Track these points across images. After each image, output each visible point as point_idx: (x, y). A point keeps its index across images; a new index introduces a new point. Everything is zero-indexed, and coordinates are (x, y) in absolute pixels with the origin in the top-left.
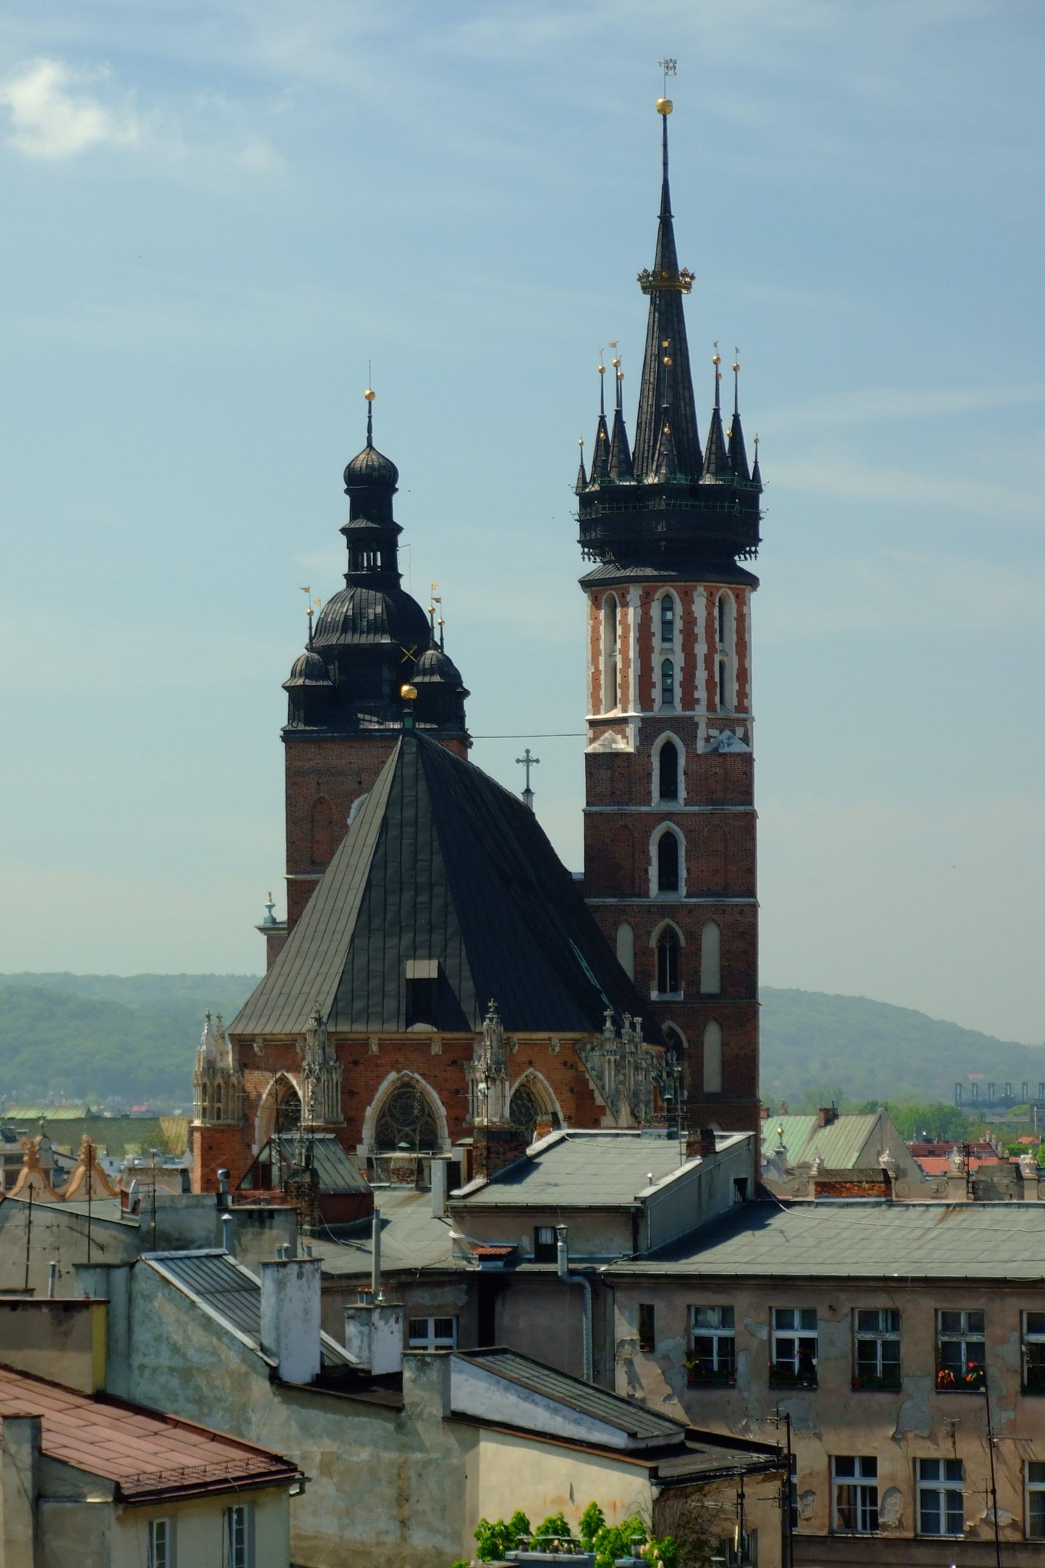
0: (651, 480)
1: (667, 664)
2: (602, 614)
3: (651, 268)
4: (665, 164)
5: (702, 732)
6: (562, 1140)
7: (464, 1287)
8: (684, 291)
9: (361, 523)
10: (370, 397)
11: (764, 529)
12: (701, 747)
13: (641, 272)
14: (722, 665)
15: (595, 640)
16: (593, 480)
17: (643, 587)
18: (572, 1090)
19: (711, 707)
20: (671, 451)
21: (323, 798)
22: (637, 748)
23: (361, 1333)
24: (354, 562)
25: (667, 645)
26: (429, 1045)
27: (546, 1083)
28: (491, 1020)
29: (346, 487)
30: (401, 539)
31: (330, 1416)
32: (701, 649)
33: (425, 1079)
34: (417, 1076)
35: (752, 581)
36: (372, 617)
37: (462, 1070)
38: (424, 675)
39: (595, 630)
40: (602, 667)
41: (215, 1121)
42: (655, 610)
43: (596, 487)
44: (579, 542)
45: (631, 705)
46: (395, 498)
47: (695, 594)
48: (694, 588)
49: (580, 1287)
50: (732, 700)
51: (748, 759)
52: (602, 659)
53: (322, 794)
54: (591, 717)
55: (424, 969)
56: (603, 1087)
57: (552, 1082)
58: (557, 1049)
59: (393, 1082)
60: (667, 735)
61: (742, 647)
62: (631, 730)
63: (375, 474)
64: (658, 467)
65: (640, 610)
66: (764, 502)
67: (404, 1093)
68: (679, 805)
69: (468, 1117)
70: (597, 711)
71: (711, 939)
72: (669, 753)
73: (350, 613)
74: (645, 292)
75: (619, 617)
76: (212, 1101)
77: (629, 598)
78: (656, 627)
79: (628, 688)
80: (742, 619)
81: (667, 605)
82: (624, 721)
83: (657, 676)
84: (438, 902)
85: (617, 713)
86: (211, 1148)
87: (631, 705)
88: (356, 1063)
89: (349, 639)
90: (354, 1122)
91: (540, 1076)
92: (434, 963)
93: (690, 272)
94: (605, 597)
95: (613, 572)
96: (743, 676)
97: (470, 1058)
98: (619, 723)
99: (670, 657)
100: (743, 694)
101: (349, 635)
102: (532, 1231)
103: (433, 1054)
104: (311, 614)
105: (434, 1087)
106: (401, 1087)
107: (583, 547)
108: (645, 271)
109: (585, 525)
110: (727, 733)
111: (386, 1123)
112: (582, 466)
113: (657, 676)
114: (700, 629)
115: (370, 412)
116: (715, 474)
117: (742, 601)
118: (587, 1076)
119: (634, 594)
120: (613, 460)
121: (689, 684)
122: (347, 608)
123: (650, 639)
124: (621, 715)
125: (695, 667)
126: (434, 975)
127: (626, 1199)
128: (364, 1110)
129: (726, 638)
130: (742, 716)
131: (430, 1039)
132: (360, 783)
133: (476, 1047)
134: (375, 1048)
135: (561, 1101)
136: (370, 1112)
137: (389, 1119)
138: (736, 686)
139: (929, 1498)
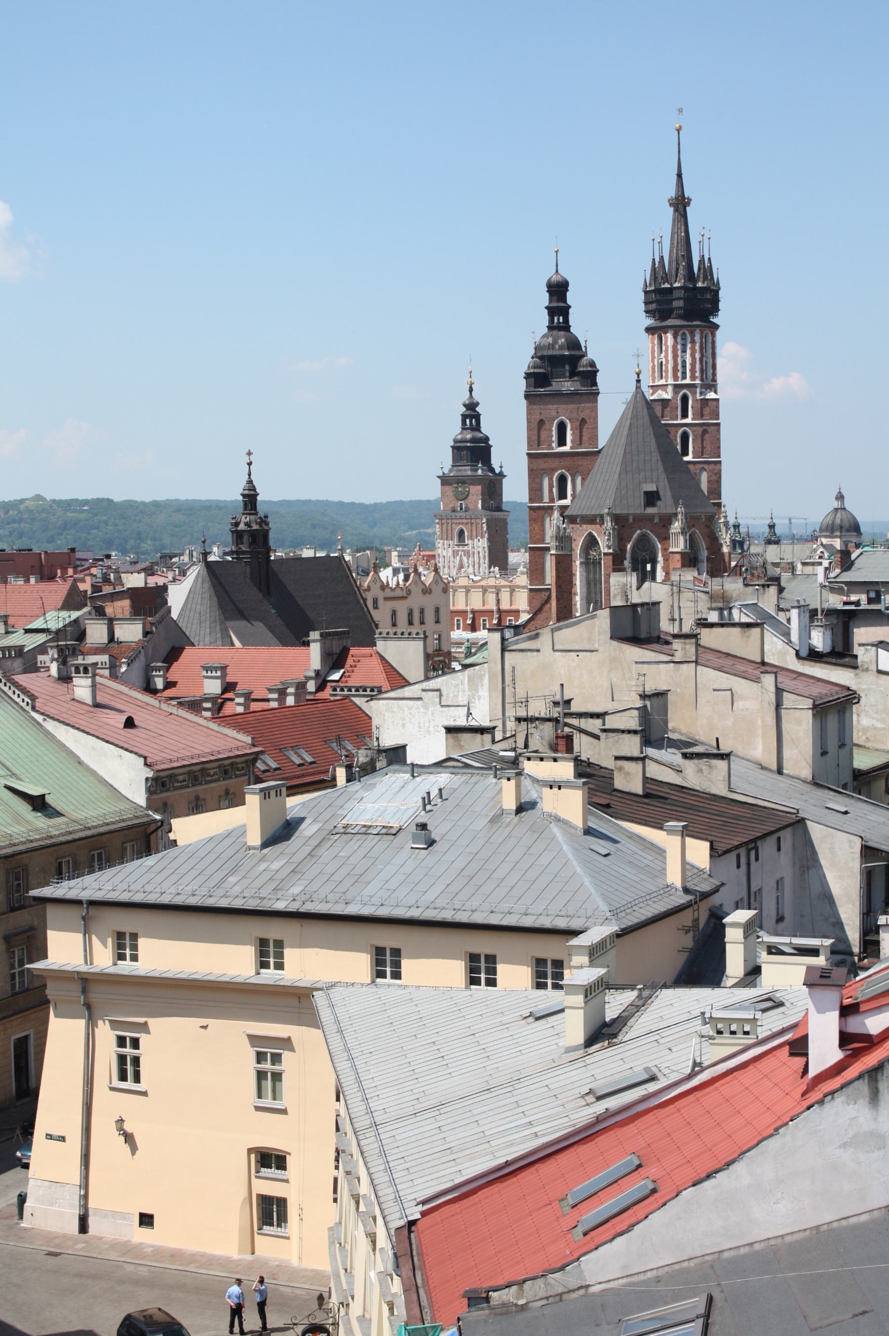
0: (676, 285)
1: (684, 362)
4: (679, 152)
6: (861, 554)
7: (836, 616)
11: (721, 305)
13: (670, 197)
15: (653, 352)
19: (702, 380)
24: (551, 321)
25: (684, 354)
26: (653, 519)
30: (571, 311)
31: (824, 671)
34: (649, 532)
35: (716, 327)
36: (560, 343)
39: (653, 348)
40: (656, 364)
43: (653, 288)
46: (568, 294)
48: (695, 330)
50: (710, 377)
52: (656, 360)
54: (651, 384)
55: (652, 488)
57: (701, 534)
62: (670, 389)
65: (673, 340)
66: (721, 294)
67: (643, 538)
68: (689, 420)
71: (704, 477)
75: (663, 342)
80: (713, 343)
82: (667, 385)
83: (680, 367)
84: (654, 459)
85: (663, 382)
88: (623, 526)
89: (551, 352)
90: (623, 550)
98: (664, 387)
100: (714, 374)
101: (551, 350)
104: (535, 343)
105: (656, 536)
109: (646, 303)
113: (680, 367)
116: (703, 282)
117: (713, 335)
122: (550, 340)
124: (665, 383)
125: (696, 363)
126: (655, 490)
133: (673, 519)
134: (631, 520)
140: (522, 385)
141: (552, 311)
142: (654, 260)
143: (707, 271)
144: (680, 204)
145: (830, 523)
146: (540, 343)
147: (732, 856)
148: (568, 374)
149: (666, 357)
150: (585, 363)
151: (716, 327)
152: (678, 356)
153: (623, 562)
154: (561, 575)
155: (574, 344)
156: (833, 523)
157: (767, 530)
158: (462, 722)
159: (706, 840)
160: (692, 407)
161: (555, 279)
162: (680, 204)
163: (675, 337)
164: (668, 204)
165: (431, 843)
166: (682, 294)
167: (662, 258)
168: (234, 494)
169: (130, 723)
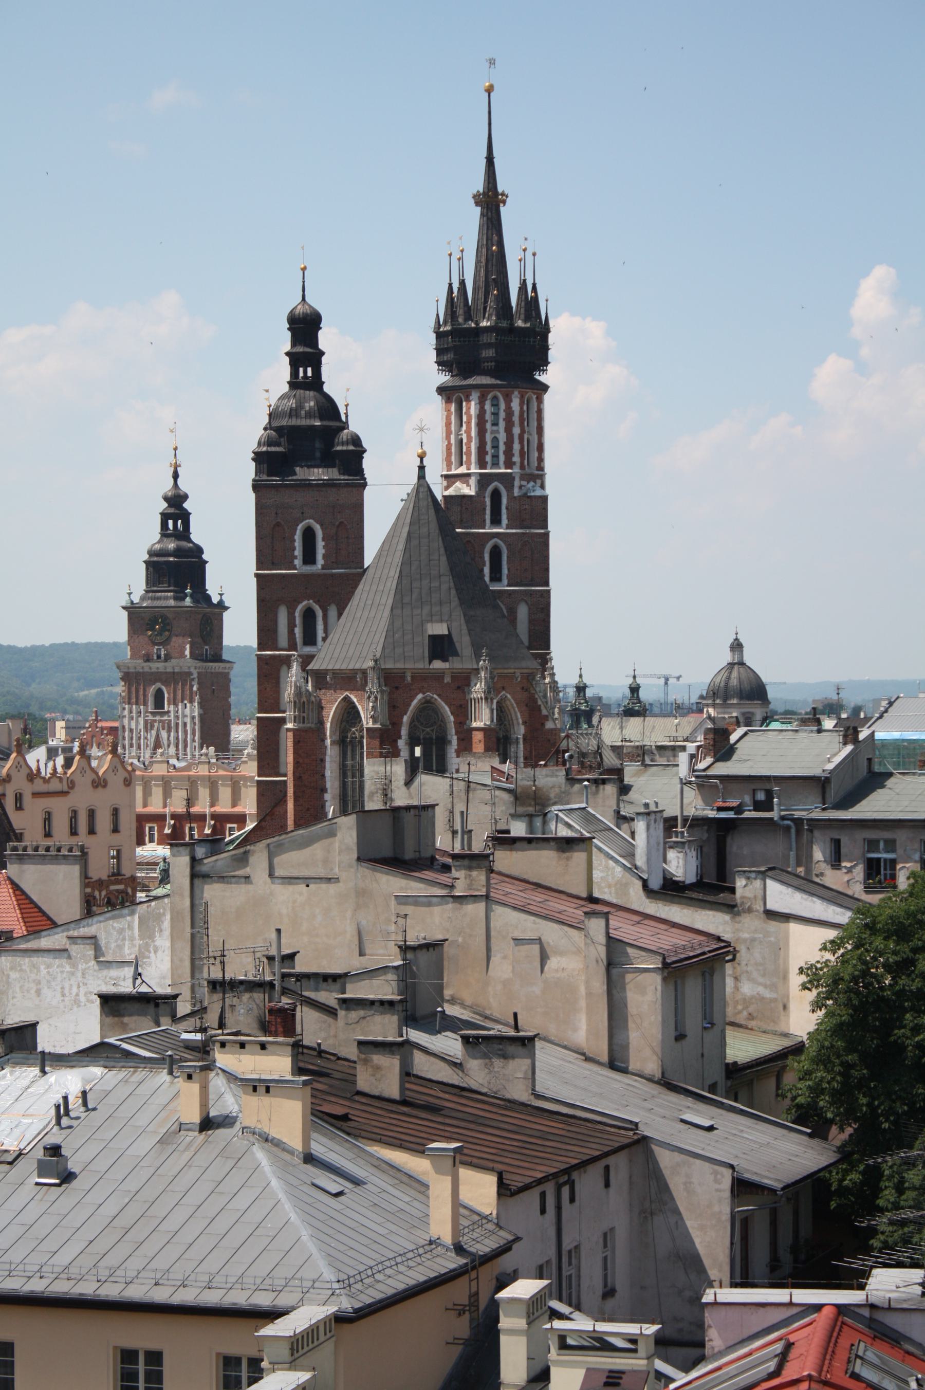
0: (484, 324)
1: (495, 440)
2: (453, 407)
3: (481, 191)
5: (517, 483)
6: (746, 734)
7: (706, 828)
8: (501, 205)
9: (300, 349)
11: (552, 354)
12: (516, 492)
13: (475, 192)
14: (528, 441)
15: (448, 424)
16: (445, 322)
17: (481, 392)
18: (527, 705)
19: (522, 467)
20: (498, 305)
21: (278, 522)
22: (476, 492)
23: (678, 857)
24: (294, 373)
25: (495, 428)
27: (512, 701)
28: (484, 661)
29: (288, 326)
31: (685, 911)
32: (516, 430)
33: (441, 698)
34: (435, 696)
35: (545, 388)
36: (307, 408)
37: (464, 692)
38: (343, 445)
40: (453, 441)
41: (301, 725)
42: (488, 406)
43: (448, 328)
44: (436, 362)
45: (473, 466)
47: (513, 396)
48: (513, 393)
49: (788, 828)
51: (545, 499)
52: (453, 437)
53: (279, 520)
54: (445, 473)
55: (440, 629)
56: (547, 702)
57: (515, 700)
58: (519, 679)
59: (420, 700)
60: (496, 484)
62: (473, 481)
63: (309, 318)
64: (490, 315)
65: (478, 406)
66: (551, 338)
67: (427, 704)
69: (468, 722)
70: (449, 469)
71: (523, 612)
72: (496, 495)
73: (294, 405)
74: (476, 205)
75: (464, 410)
76: (299, 711)
77: (471, 398)
78: (488, 416)
79: (471, 455)
80: (540, 412)
81: (495, 404)
82: (468, 475)
84: (445, 587)
85: (463, 470)
86: (299, 742)
87: (473, 466)
88: (397, 688)
89: (294, 422)
90: (395, 724)
91: (509, 696)
92: (445, 626)
93: (506, 193)
94: (454, 397)
95: (458, 382)
97: (468, 685)
98: (464, 477)
99: (497, 435)
100: (541, 459)
101: (294, 419)
102: (751, 793)
103: (446, 681)
104: (270, 406)
105: (446, 703)
106: (425, 703)
107: (439, 365)
108: (478, 192)
109: (440, 351)
110: (532, 484)
111: (415, 726)
112: (438, 315)
113: (488, 447)
114: (516, 418)
115: (304, 278)
116: (525, 321)
117: (540, 401)
118: (536, 696)
119: (475, 396)
120: (460, 311)
121: (509, 453)
122: (292, 403)
123: (485, 425)
125: (512, 442)
126: (446, 632)
127: (816, 771)
128: (402, 718)
129: (531, 424)
130: (540, 473)
131: (444, 673)
132: (303, 513)
133: (473, 677)
134: (409, 679)
135: (521, 712)
136: (405, 719)
137: (417, 723)
138: (536, 454)
140: (249, 470)
141: (295, 360)
142: (450, 285)
143: (531, 305)
145: (722, 684)
146: (278, 407)
147: (533, 1197)
148: (318, 454)
149: (468, 432)
150: (345, 439)
151: (545, 388)
152: (486, 431)
153: (396, 741)
154: (301, 761)
155: (329, 408)
156: (727, 683)
157: (628, 692)
158: (126, 987)
159: (492, 1170)
160: (507, 508)
161: (300, 310)
163: (481, 403)
164: (472, 201)
165: (67, 1177)
167: (462, 283)
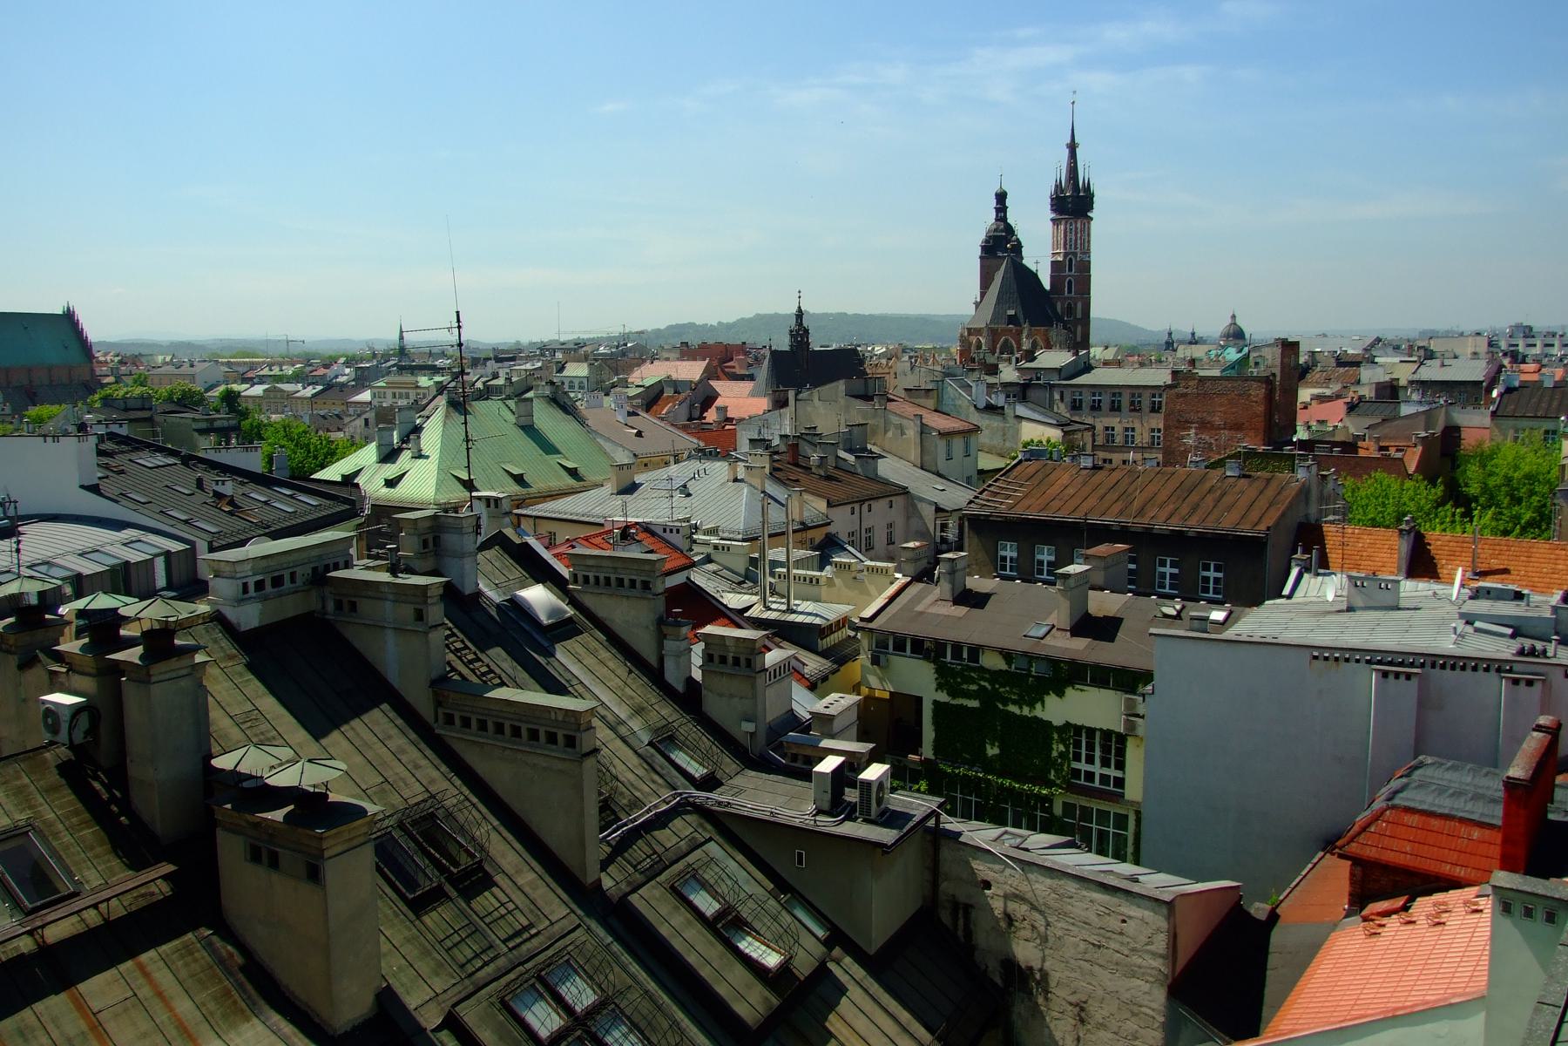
10: (1073, 103)
24: (997, 215)
32: (1079, 235)
35: (1092, 219)
51: (1089, 262)
55: (1011, 312)
61: (1089, 235)
67: (1007, 340)
71: (1079, 305)
72: (1071, 260)
80: (1089, 228)
90: (995, 348)
96: (1089, 242)
100: (1089, 246)
109: (1052, 206)
117: (1089, 223)
119: (1063, 222)
127: (1058, 367)
139: (1127, 436)
140: (978, 252)
141: (998, 210)
143: (1087, 188)
144: (1072, 147)
147: (848, 508)
151: (1092, 219)
155: (1009, 230)
158: (756, 437)
159: (824, 497)
162: (1072, 147)
163: (1066, 225)
165: (689, 495)
166: (1070, 200)
168: (794, 310)
169: (639, 434)
